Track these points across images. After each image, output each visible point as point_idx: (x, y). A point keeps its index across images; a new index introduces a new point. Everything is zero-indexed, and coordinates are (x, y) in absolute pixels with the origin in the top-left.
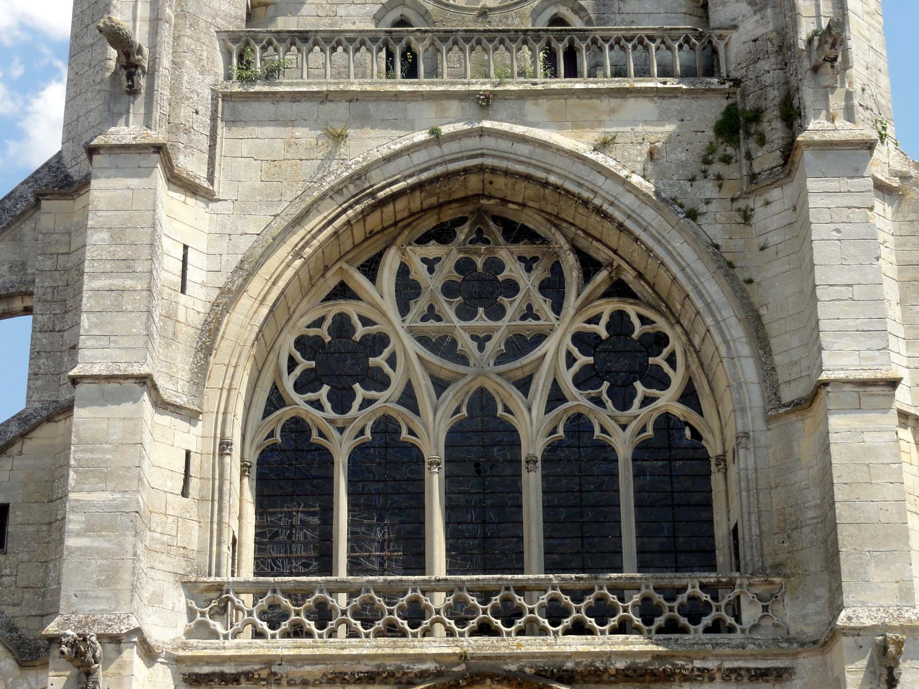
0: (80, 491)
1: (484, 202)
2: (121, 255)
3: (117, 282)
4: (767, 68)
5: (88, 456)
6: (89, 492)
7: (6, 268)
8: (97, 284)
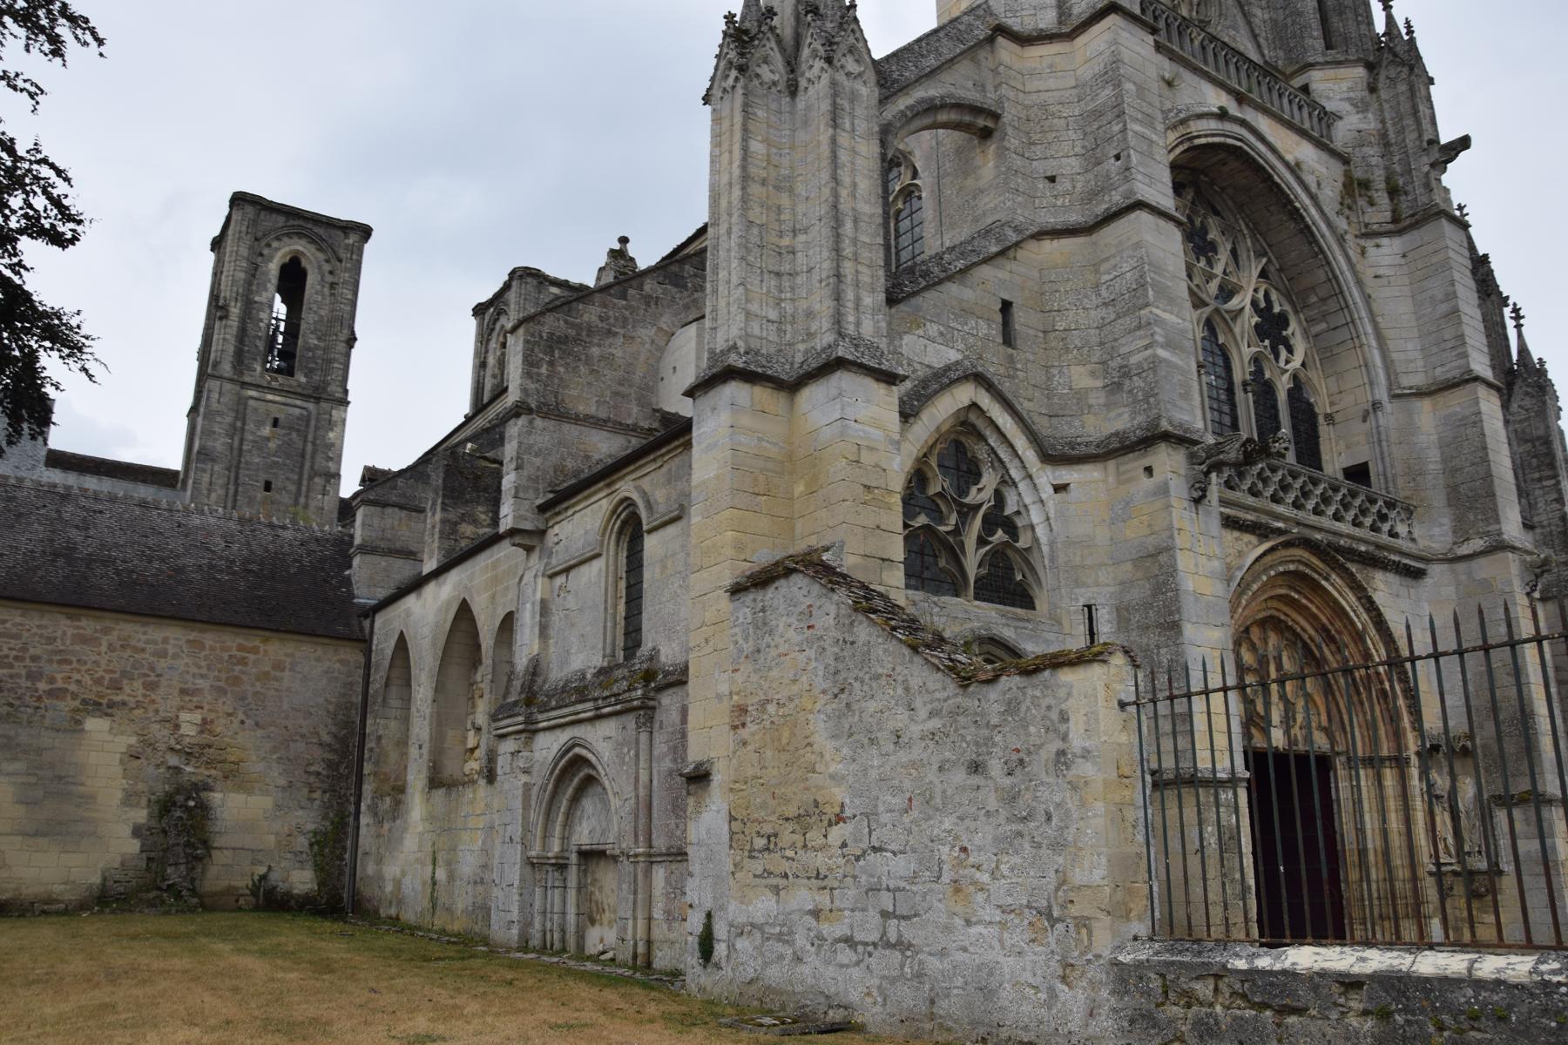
0: (1157, 307)
1: (1202, 177)
2: (1144, 110)
3: (1147, 132)
4: (1371, 153)
5: (1157, 277)
6: (1165, 311)
7: (970, 84)
8: (1137, 127)
